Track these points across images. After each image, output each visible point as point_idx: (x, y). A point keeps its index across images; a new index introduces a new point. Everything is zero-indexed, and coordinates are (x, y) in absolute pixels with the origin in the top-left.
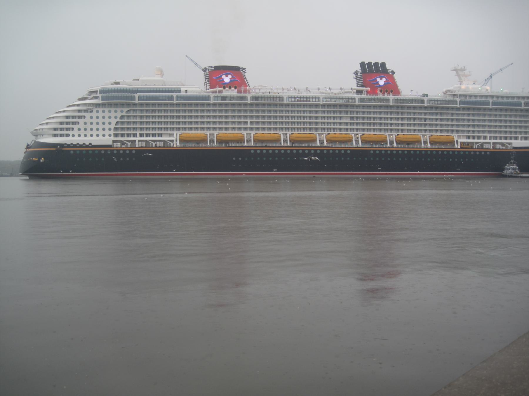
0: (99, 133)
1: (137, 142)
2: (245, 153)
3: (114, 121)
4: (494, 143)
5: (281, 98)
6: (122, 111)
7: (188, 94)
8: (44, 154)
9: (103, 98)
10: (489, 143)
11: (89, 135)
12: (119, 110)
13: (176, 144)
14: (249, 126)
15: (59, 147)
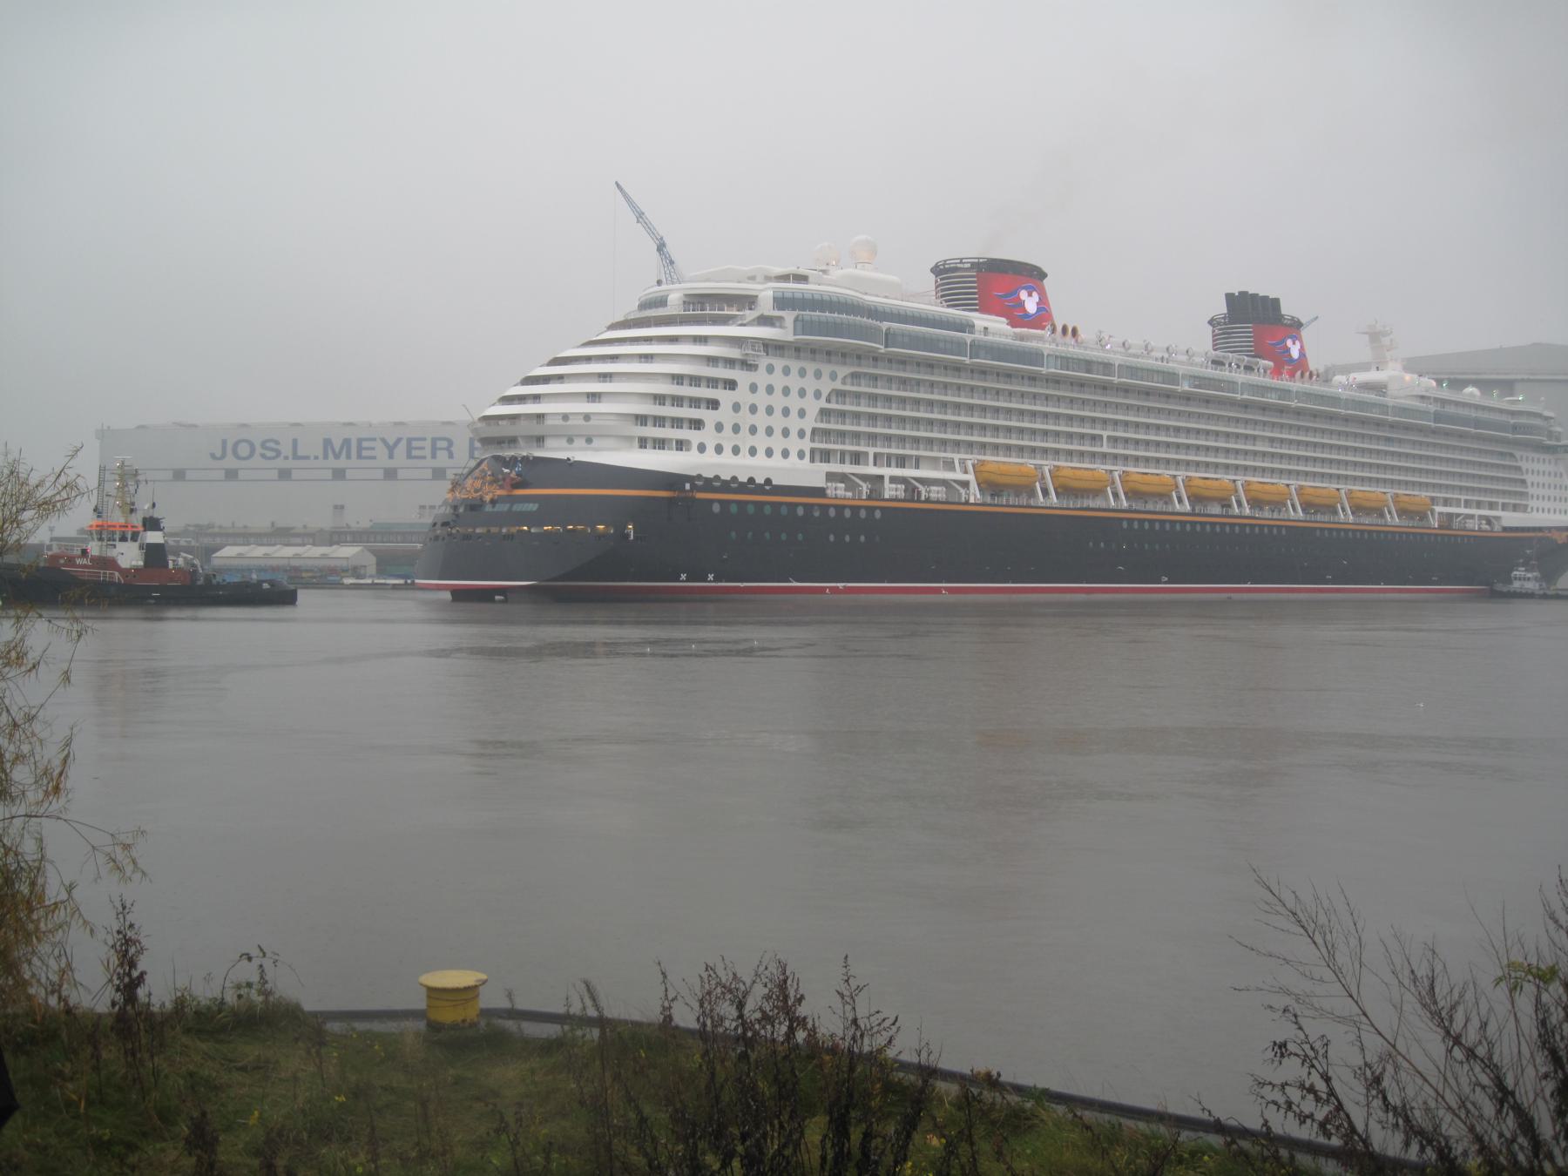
0: (765, 444)
1: (887, 480)
2: (1104, 526)
3: (813, 407)
4: (1481, 517)
5: (1172, 377)
6: (833, 376)
7: (990, 338)
8: (638, 510)
9: (802, 326)
10: (1472, 517)
11: (745, 450)
12: (827, 369)
13: (974, 495)
14: (1105, 449)
15: (688, 486)
